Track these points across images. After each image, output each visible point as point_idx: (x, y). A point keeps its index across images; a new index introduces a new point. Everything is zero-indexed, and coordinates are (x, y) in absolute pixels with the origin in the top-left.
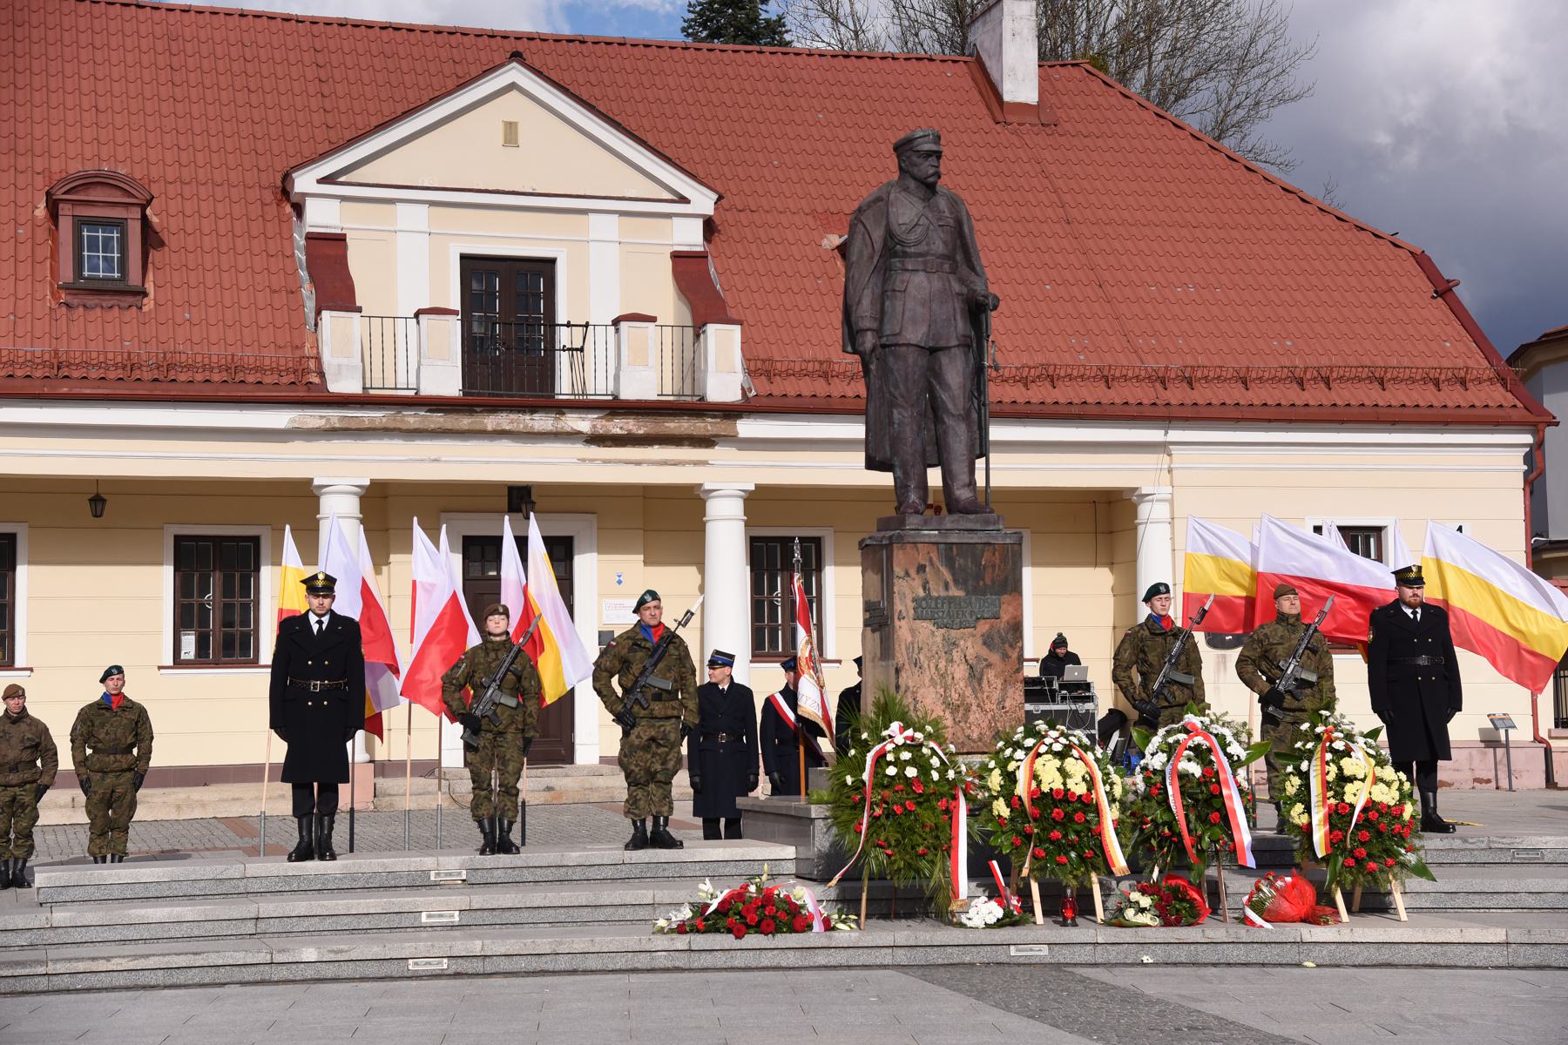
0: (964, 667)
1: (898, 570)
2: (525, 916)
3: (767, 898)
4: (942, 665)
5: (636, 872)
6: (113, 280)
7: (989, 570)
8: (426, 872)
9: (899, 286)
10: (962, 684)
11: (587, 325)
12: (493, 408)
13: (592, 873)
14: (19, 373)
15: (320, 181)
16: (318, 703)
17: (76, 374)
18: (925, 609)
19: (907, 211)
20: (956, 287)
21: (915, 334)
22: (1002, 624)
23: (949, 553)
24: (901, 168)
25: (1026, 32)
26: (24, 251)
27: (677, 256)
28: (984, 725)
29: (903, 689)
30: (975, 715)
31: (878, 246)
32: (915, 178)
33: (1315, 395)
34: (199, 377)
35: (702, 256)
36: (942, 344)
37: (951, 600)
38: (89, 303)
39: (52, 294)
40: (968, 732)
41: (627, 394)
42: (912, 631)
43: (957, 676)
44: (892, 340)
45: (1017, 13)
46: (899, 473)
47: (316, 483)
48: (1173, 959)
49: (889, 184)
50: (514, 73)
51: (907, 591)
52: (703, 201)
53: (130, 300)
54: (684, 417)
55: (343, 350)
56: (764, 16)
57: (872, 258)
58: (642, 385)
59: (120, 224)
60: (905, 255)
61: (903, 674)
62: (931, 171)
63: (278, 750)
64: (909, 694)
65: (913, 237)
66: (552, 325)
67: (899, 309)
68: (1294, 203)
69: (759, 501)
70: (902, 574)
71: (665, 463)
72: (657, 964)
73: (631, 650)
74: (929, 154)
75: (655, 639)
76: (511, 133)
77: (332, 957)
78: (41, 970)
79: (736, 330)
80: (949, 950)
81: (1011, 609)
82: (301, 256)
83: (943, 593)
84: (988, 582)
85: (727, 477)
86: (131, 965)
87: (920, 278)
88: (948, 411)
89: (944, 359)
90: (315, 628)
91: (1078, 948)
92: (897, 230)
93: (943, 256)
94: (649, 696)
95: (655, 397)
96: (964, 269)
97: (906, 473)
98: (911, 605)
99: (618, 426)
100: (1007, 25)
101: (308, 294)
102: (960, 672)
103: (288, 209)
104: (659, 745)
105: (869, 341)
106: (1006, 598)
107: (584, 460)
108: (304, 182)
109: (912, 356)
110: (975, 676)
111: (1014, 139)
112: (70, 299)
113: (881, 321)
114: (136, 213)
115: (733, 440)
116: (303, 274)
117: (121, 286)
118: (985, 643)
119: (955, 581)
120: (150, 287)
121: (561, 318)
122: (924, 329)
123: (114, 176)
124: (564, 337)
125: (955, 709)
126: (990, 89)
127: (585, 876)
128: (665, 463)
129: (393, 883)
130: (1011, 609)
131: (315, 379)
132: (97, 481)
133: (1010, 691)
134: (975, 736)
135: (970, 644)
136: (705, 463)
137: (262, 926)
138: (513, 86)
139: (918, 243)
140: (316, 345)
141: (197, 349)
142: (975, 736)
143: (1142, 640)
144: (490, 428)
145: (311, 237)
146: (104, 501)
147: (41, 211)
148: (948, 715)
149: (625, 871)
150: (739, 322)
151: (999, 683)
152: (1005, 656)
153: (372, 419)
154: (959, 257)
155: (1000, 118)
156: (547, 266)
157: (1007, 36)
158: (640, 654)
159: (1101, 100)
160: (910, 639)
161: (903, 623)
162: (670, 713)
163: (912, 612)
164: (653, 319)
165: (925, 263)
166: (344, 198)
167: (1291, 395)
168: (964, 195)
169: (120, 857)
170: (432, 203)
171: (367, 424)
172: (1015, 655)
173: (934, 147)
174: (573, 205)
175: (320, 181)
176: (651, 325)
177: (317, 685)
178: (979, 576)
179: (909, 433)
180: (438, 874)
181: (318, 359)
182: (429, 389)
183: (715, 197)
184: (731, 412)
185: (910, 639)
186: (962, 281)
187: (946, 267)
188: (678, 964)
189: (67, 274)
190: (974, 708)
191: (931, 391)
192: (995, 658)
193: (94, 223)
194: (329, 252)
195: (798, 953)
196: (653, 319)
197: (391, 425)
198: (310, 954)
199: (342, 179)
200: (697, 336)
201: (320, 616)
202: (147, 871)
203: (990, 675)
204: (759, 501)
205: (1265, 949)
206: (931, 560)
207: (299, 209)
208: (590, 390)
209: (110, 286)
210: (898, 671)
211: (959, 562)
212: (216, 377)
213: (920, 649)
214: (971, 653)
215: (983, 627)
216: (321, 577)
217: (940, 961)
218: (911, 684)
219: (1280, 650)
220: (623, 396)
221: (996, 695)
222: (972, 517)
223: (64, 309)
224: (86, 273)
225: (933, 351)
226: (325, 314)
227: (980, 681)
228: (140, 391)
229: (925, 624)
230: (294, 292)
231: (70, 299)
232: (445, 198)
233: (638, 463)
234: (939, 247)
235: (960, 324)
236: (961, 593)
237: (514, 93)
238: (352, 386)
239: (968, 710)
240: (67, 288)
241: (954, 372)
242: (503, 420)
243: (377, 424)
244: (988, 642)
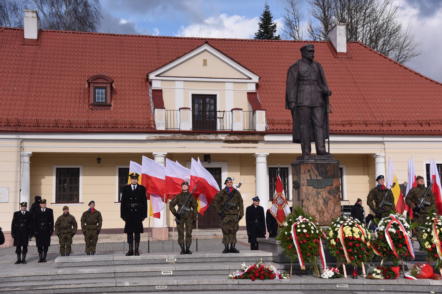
0: (322, 200)
1: (302, 171)
2: (192, 273)
3: (262, 268)
4: (316, 199)
5: (226, 260)
6: (103, 102)
8: (165, 259)
9: (302, 89)
10: (322, 205)
11: (224, 111)
12: (199, 133)
14: (79, 126)
15: (156, 76)
17: (93, 126)
18: (310, 183)
19: (304, 68)
20: (319, 89)
21: (307, 103)
22: (333, 187)
23: (317, 166)
24: (302, 56)
25: (343, 34)
26: (82, 96)
27: (248, 93)
29: (304, 206)
30: (326, 214)
31: (296, 78)
32: (306, 58)
33: (425, 128)
34: (123, 127)
35: (255, 93)
36: (315, 106)
38: (97, 108)
39: (88, 106)
40: (324, 219)
41: (235, 129)
42: (307, 189)
43: (320, 203)
44: (300, 105)
45: (341, 29)
46: (302, 143)
48: (388, 290)
49: (299, 60)
50: (206, 47)
51: (305, 178)
52: (256, 79)
53: (107, 107)
54: (250, 135)
55: (160, 119)
56: (274, 35)
57: (294, 81)
58: (239, 127)
60: (304, 80)
61: (304, 202)
62: (311, 56)
63: (122, 224)
64: (306, 208)
65: (306, 75)
66: (215, 111)
67: (302, 96)
68: (418, 77)
69: (271, 158)
70: (303, 172)
71: (245, 148)
72: (229, 288)
73: (223, 195)
74: (311, 51)
75: (231, 192)
76: (205, 62)
77: (134, 285)
78: (51, 288)
79: (264, 112)
80: (318, 285)
81: (336, 183)
82: (151, 95)
83: (316, 178)
84: (329, 175)
85: (262, 151)
86: (76, 287)
87: (308, 87)
88: (317, 125)
89: (315, 110)
90: (133, 189)
91: (358, 285)
92: (302, 73)
93: (315, 80)
94: (229, 208)
95: (242, 130)
96: (321, 84)
97: (304, 143)
98: (306, 182)
99: (232, 138)
100: (338, 32)
101: (152, 104)
102: (321, 201)
103: (148, 84)
104: (232, 223)
105: (293, 105)
106: (335, 179)
107: (223, 147)
109: (306, 109)
110: (326, 203)
111: (340, 62)
112: (93, 108)
113: (297, 99)
114: (109, 85)
115: (263, 141)
116: (151, 100)
117: (105, 104)
118: (328, 193)
120: (112, 104)
121: (218, 110)
122: (309, 102)
123: (104, 76)
124: (218, 115)
125: (319, 212)
126: (333, 49)
128: (245, 148)
129: (155, 262)
130: (336, 183)
131: (153, 126)
132: (99, 154)
133: (336, 207)
134: (326, 220)
135: (324, 193)
136: (256, 148)
137: (116, 275)
138: (206, 50)
139: (307, 77)
140: (154, 118)
141: (123, 119)
142: (326, 220)
143: (376, 192)
145: (154, 91)
146: (100, 159)
147: (87, 86)
148: (318, 214)
150: (265, 110)
151: (333, 205)
152: (335, 197)
153: (167, 137)
154: (320, 81)
155: (336, 56)
156: (214, 97)
157: (338, 35)
158: (226, 196)
159: (364, 51)
160: (306, 192)
161: (304, 187)
162: (235, 213)
163: (306, 184)
164: (242, 110)
165: (309, 82)
167: (419, 128)
168: (319, 62)
169: (93, 254)
170: (185, 81)
171: (166, 138)
172: (337, 197)
173: (312, 49)
174: (220, 81)
175: (156, 76)
176: (241, 111)
177: (133, 205)
179: (305, 132)
180: (168, 260)
181: (154, 121)
182: (182, 129)
183: (259, 78)
184: (262, 134)
185: (306, 192)
186: (321, 88)
187: (316, 83)
188: (235, 288)
189: (92, 101)
190: (325, 212)
191: (311, 119)
192: (331, 197)
194: (158, 94)
195: (271, 286)
196: (242, 110)
197: (173, 138)
198: (127, 284)
199: (162, 75)
200: (254, 114)
201: (134, 185)
202: (86, 258)
203: (330, 202)
204: (271, 158)
205: (418, 287)
206: (312, 168)
207: (151, 84)
208: (225, 128)
209: (102, 104)
210: (302, 201)
211: (320, 169)
212: (128, 127)
213: (309, 195)
214: (324, 196)
215: (328, 188)
216: (135, 174)
217: (315, 289)
218: (306, 205)
219: (419, 195)
220: (234, 130)
221: (332, 208)
222: (324, 156)
223: (91, 110)
224: (97, 101)
225: (312, 108)
226: (156, 110)
227: (327, 204)
229: (310, 187)
230: (149, 104)
231: (93, 108)
232: (188, 80)
233: (238, 148)
234: (313, 78)
235: (320, 100)
237: (206, 52)
238: (162, 128)
239: (324, 213)
240: (93, 105)
241: (319, 114)
242: (202, 137)
243: (169, 138)
244: (329, 192)
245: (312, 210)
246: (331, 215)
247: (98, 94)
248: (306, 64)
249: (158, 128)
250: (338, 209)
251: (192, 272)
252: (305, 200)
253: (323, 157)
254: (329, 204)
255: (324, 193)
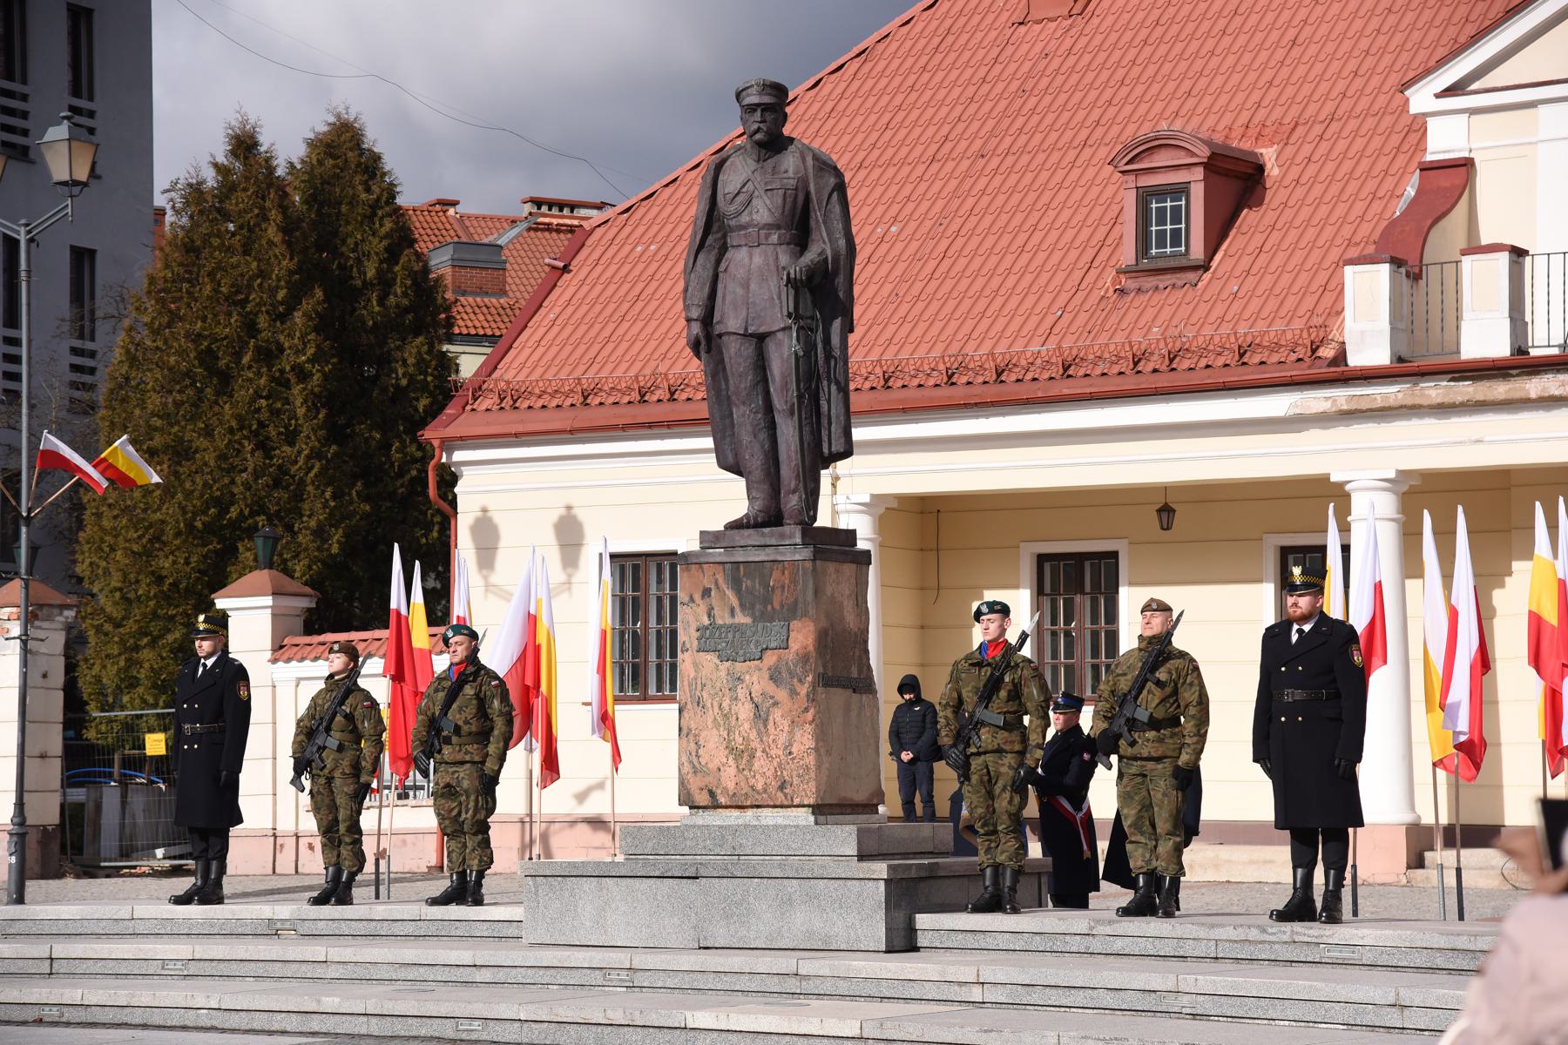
0: (749, 706)
1: (682, 595)
2: (234, 969)
4: (725, 705)
5: (432, 930)
7: (778, 592)
10: (747, 726)
13: (398, 929)
16: (191, 747)
23: (737, 573)
28: (769, 774)
29: (685, 731)
30: (760, 763)
36: (762, 330)
37: (736, 628)
42: (696, 665)
43: (741, 717)
47: (1332, 479)
51: (691, 618)
59: (1181, 190)
60: (732, 230)
61: (685, 714)
64: (691, 737)
65: (732, 208)
70: (686, 599)
83: (729, 621)
84: (777, 606)
93: (769, 226)
102: (745, 711)
106: (795, 624)
108: (1421, 98)
110: (760, 717)
114: (1199, 173)
117: (1183, 262)
119: (742, 605)
127: (272, 930)
129: (240, 931)
130: (800, 637)
132: (1165, 489)
133: (798, 736)
134: (759, 787)
135: (756, 679)
142: (759, 787)
144: (1533, 395)
148: (731, 762)
149: (423, 929)
152: (793, 693)
153: (1385, 396)
163: (696, 643)
166: (1473, 111)
171: (1379, 403)
178: (767, 600)
188: (215, 1023)
190: (759, 754)
192: (782, 695)
193: (1161, 192)
197: (1409, 402)
199: (1474, 87)
202: (107, 908)
203: (777, 714)
206: (716, 583)
211: (746, 583)
214: (756, 690)
215: (770, 659)
217: (402, 1033)
218: (693, 726)
221: (783, 739)
227: (766, 722)
228: (1146, 382)
231: (1131, 284)
234: (763, 211)
236: (748, 620)
243: (1392, 402)
244: (775, 677)
245: (711, 745)
246: (780, 764)
247: (1161, 221)
248: (750, 161)
249: (1356, 360)
250: (805, 740)
251: (234, 965)
252: (689, 706)
253: (763, 535)
254: (771, 726)
255: (755, 679)
